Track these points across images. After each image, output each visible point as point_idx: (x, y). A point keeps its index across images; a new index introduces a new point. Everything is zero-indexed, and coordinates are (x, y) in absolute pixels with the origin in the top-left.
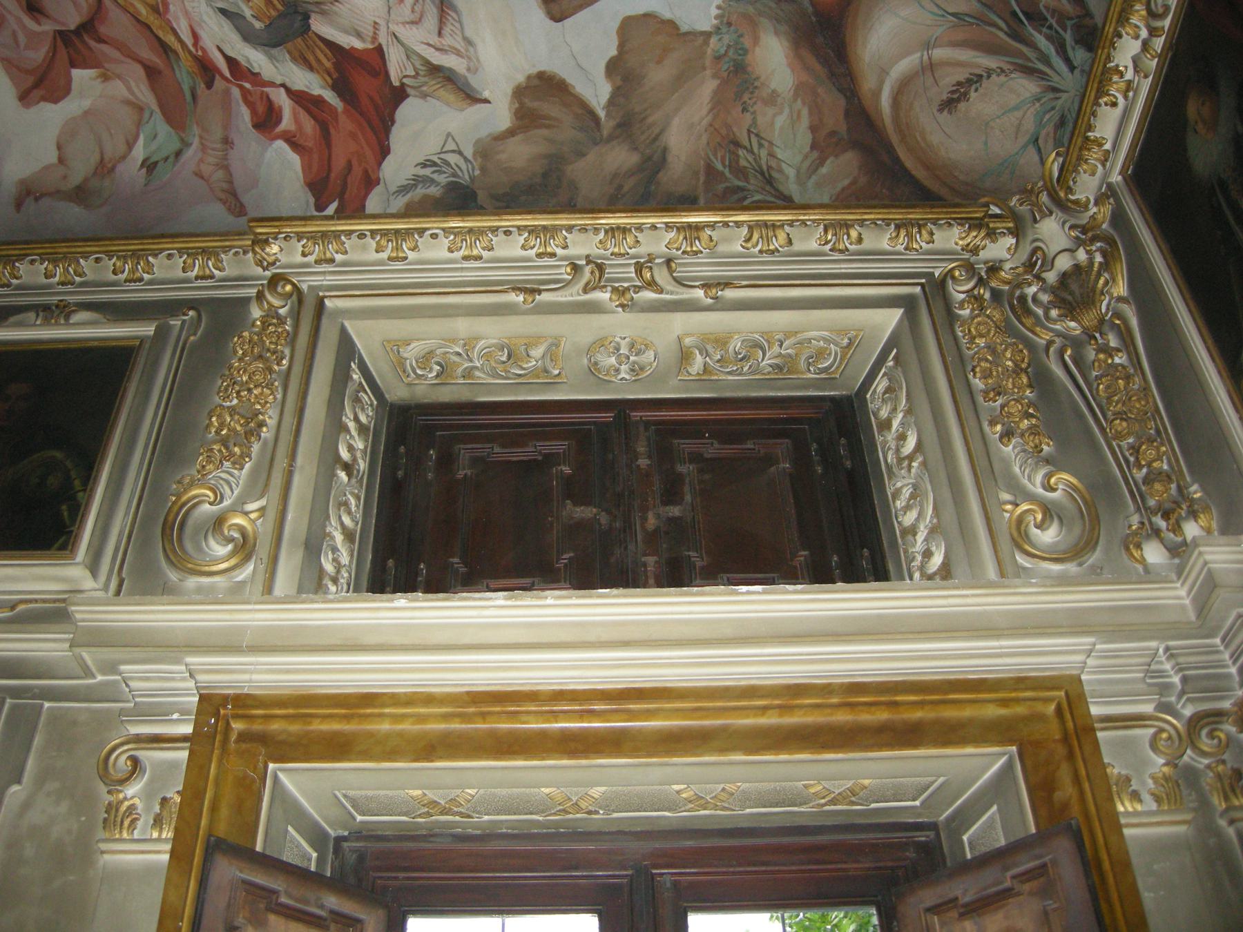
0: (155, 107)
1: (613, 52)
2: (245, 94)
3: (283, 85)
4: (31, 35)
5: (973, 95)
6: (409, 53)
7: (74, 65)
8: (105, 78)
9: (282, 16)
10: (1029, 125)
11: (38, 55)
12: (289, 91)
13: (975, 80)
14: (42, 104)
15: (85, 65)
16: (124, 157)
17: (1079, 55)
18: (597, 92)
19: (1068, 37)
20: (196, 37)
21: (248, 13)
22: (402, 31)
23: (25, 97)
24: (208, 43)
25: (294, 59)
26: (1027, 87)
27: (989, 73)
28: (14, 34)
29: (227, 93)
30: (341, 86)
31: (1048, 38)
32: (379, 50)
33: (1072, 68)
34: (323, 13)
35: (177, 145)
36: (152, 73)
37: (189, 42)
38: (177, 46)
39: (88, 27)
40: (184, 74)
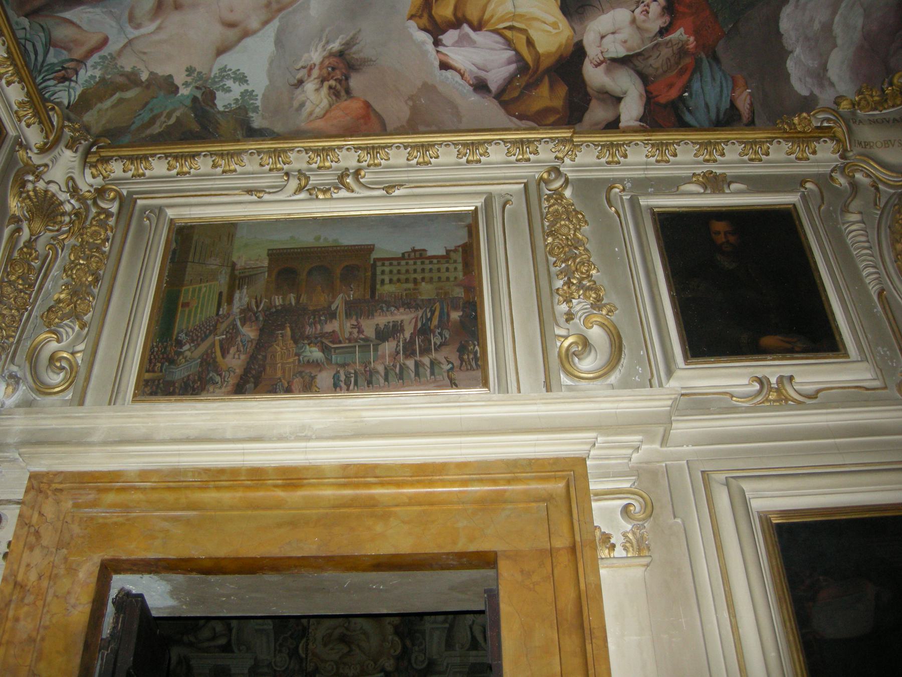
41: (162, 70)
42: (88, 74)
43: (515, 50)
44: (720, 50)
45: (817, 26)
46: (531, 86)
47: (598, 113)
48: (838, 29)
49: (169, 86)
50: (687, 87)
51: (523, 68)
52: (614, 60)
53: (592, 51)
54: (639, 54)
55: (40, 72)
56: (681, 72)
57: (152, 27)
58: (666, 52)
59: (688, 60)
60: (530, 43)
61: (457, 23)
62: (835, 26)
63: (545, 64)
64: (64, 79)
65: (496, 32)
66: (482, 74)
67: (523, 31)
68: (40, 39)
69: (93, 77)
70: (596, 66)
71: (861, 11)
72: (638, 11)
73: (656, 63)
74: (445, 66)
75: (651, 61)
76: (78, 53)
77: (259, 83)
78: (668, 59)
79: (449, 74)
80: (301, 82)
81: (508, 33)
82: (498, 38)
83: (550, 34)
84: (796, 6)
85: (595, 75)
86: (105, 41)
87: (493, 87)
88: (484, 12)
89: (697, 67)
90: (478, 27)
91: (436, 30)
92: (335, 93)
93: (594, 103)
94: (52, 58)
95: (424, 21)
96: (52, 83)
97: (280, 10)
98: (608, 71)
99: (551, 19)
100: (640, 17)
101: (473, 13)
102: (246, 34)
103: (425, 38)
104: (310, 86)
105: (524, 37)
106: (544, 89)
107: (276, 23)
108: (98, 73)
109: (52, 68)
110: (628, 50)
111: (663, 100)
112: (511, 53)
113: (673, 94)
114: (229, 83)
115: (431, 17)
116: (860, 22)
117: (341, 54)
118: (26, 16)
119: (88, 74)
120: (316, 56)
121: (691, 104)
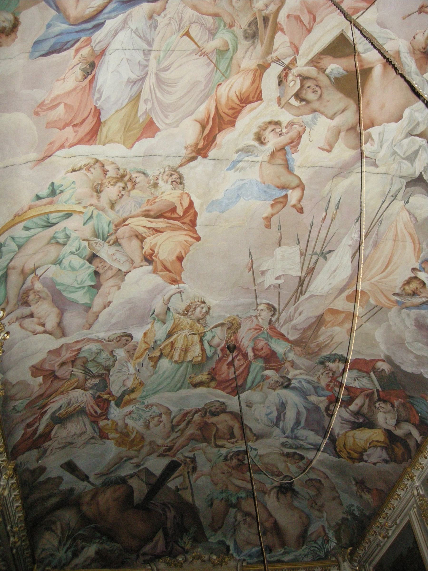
0: (32, 399)
1: (53, 477)
2: (36, 418)
3: (39, 424)
4: (54, 364)
5: (49, 532)
6: (50, 446)
7: (43, 376)
8: (40, 385)
9: (60, 418)
10: (46, 547)
11: (47, 367)
12: (38, 426)
13: (53, 531)
14: (31, 372)
15: (43, 380)
16: (16, 400)
17: (70, 554)
18: (42, 478)
19: (73, 549)
20: (53, 402)
21: (61, 411)
22: (56, 442)
23: (33, 366)
24: (51, 405)
25: (47, 424)
26: (56, 543)
27: (56, 533)
28: (54, 360)
29: (37, 414)
30: (41, 436)
31: (70, 544)
32: (51, 439)
33: (66, 552)
34: (61, 426)
35: (20, 409)
36: (41, 396)
37: (52, 401)
38: (50, 399)
39: (56, 377)
40: (41, 402)
41: (340, 518)
42: (330, 534)
43: (378, 447)
44: (408, 394)
45: (415, 360)
46: (393, 450)
47: (412, 444)
48: (420, 353)
49: (344, 520)
50: (418, 412)
51: (386, 448)
52: (396, 425)
53: (390, 428)
54: (398, 417)
55: (321, 548)
56: (412, 410)
57: (325, 514)
58: (401, 409)
59: (408, 405)
60: (378, 442)
61: (361, 454)
62: (418, 354)
63: (387, 441)
64: (328, 541)
65: (369, 448)
66: (382, 458)
67: (373, 441)
68: (312, 544)
69: (332, 533)
70: (396, 430)
71: (415, 343)
72: (381, 410)
73: (403, 414)
74: (375, 464)
75: (402, 415)
76: (323, 534)
77: (356, 504)
78: (404, 410)
79: (378, 464)
80: (361, 496)
81: (372, 445)
82: (371, 448)
83: (377, 435)
84: (403, 364)
85: (399, 432)
86: (323, 526)
87: (388, 459)
88: (360, 447)
89: (413, 404)
90: (366, 451)
91: (361, 459)
92: (369, 492)
93: (408, 441)
94: (320, 543)
95: (356, 461)
96: (327, 546)
97: (335, 488)
98: (400, 428)
99: (372, 433)
100: (384, 410)
101: (360, 450)
102: (339, 497)
103: (362, 464)
104: (363, 495)
105: (375, 442)
106: (396, 449)
107: (339, 491)
108: (332, 531)
109: (323, 544)
110: (394, 419)
111: (418, 422)
112: (379, 448)
113: (418, 418)
114: (352, 508)
115: (357, 459)
116: (420, 345)
117: (357, 483)
118: (303, 545)
119: (330, 534)
120: (355, 488)
121: (423, 416)
